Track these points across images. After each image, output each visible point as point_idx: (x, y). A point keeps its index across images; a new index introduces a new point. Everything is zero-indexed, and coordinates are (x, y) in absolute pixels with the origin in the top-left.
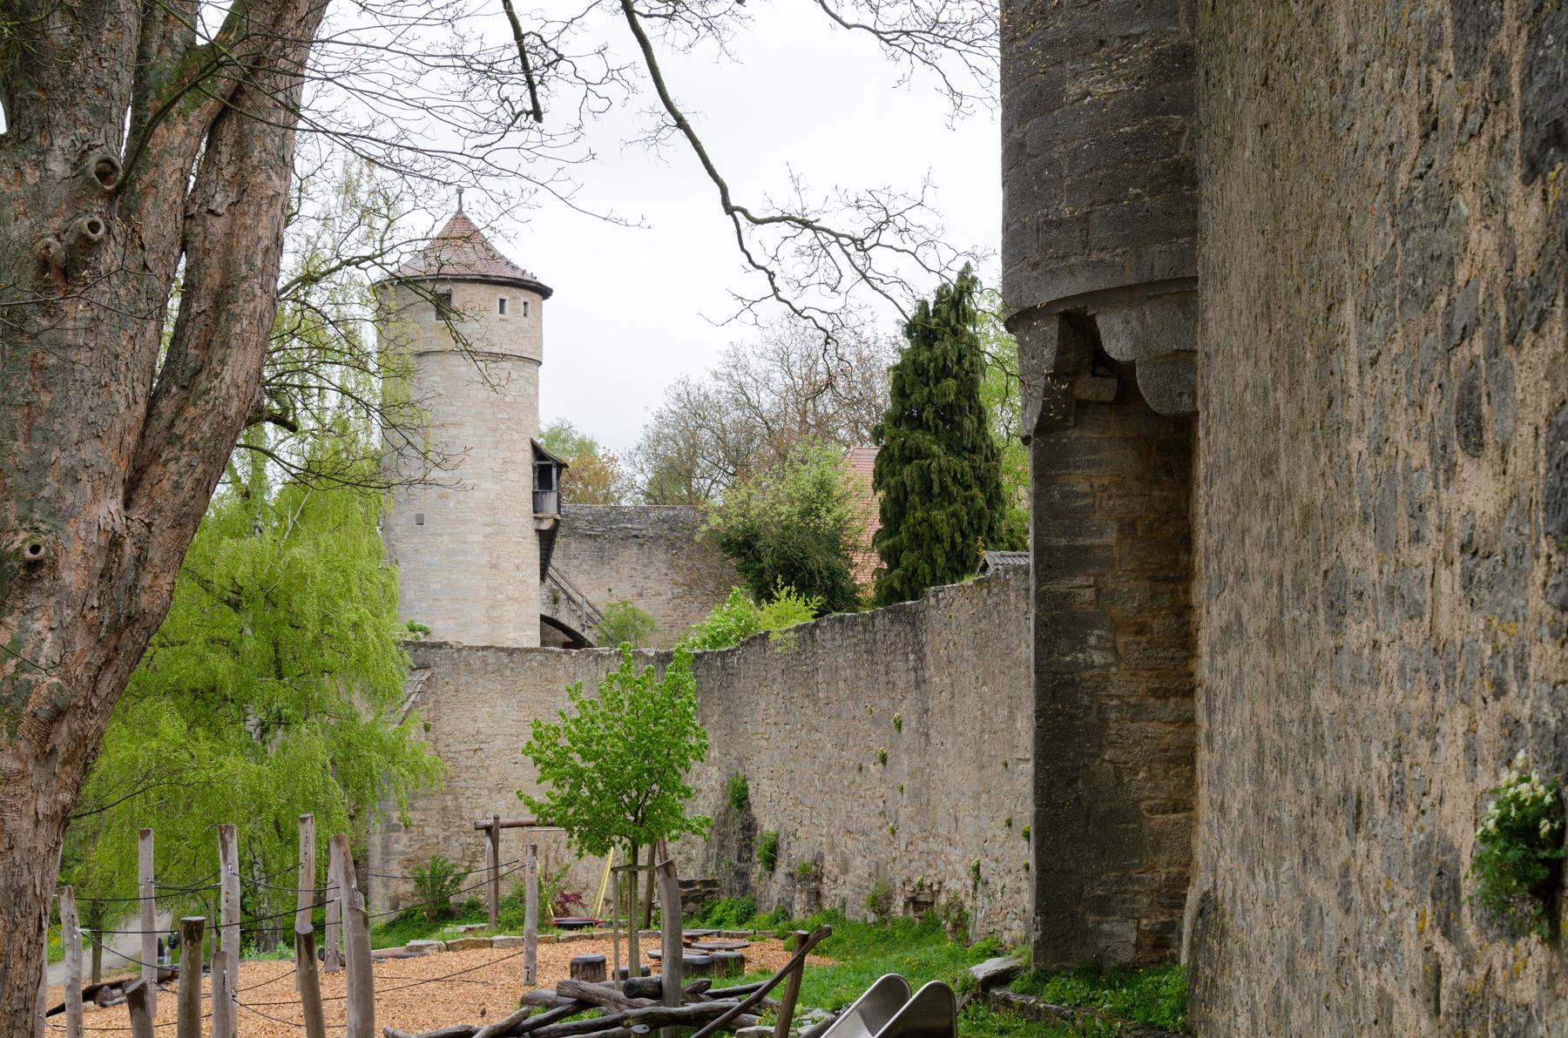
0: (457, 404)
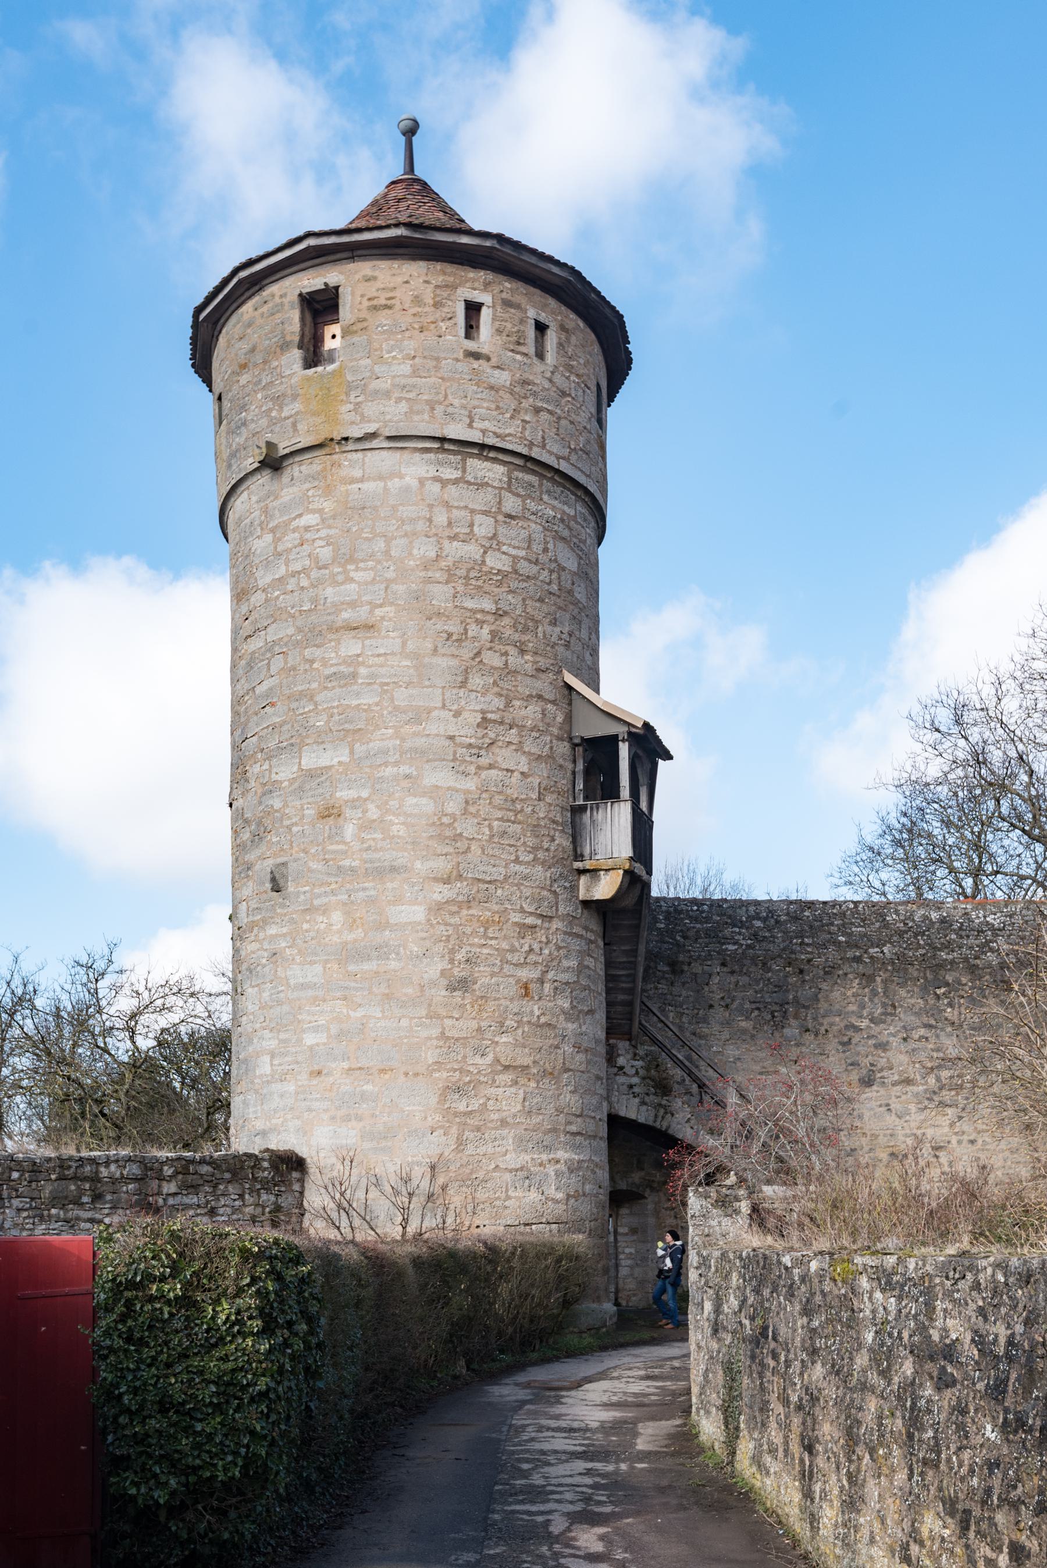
0: (358, 576)
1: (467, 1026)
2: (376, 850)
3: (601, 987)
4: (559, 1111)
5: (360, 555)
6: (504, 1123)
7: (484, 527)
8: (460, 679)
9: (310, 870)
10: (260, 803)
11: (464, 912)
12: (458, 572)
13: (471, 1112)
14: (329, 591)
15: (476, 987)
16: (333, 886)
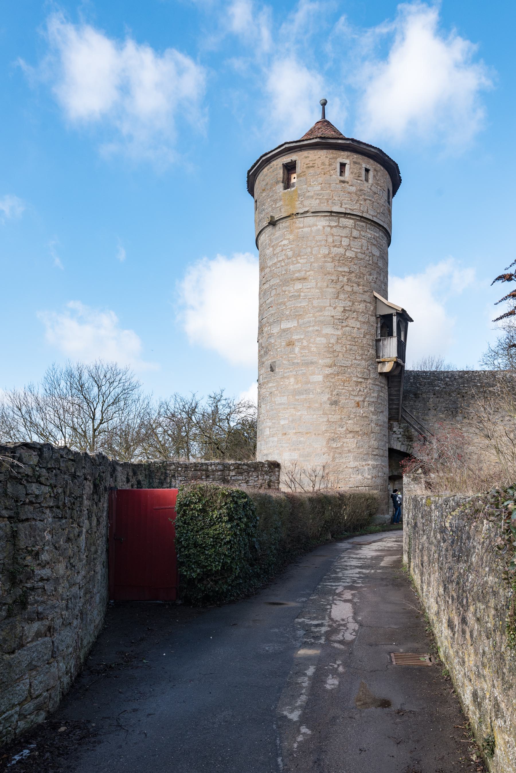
0: (301, 261)
1: (336, 417)
2: (306, 356)
3: (386, 403)
4: (369, 447)
5: (302, 254)
6: (349, 451)
7: (345, 242)
8: (336, 296)
9: (283, 364)
10: (267, 341)
11: (336, 377)
12: (336, 258)
13: (338, 448)
14: (291, 267)
15: (340, 404)
16: (291, 369)
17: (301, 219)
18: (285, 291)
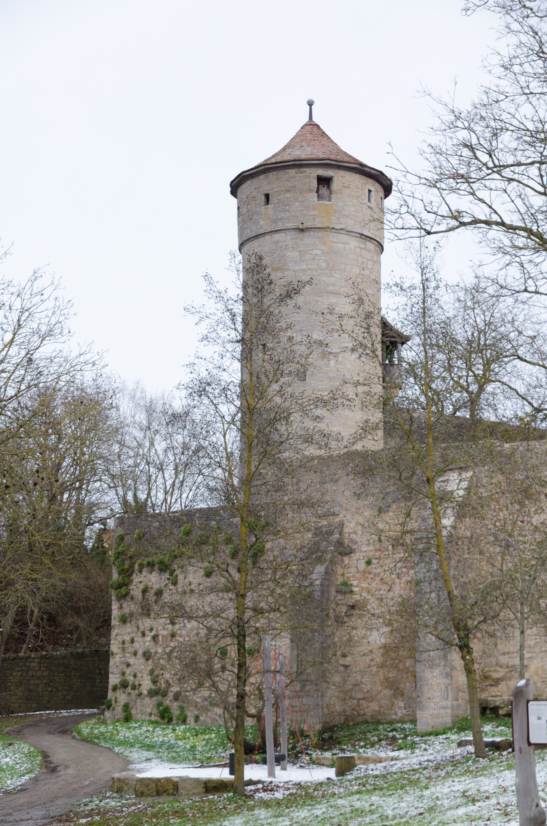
0: (336, 275)
14: (325, 278)
17: (335, 234)
18: (317, 302)
